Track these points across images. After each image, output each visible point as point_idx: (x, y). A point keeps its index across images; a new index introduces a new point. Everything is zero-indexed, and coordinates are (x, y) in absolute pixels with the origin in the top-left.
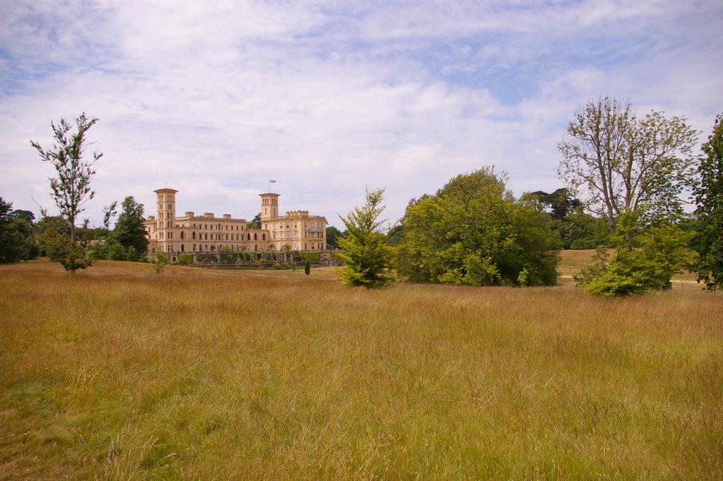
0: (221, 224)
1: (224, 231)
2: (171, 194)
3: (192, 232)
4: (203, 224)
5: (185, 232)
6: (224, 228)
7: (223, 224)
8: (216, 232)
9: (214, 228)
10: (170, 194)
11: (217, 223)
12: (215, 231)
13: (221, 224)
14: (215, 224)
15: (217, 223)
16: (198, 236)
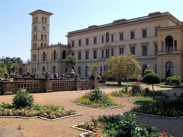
0: (111, 32)
1: (117, 42)
2: (45, 16)
3: (53, 52)
4: (83, 37)
5: (46, 53)
6: (117, 37)
7: (116, 32)
8: (103, 45)
9: (99, 40)
10: (35, 16)
11: (104, 33)
12: (100, 45)
13: (111, 32)
14: (99, 35)
15: (104, 33)
16: (59, 56)
